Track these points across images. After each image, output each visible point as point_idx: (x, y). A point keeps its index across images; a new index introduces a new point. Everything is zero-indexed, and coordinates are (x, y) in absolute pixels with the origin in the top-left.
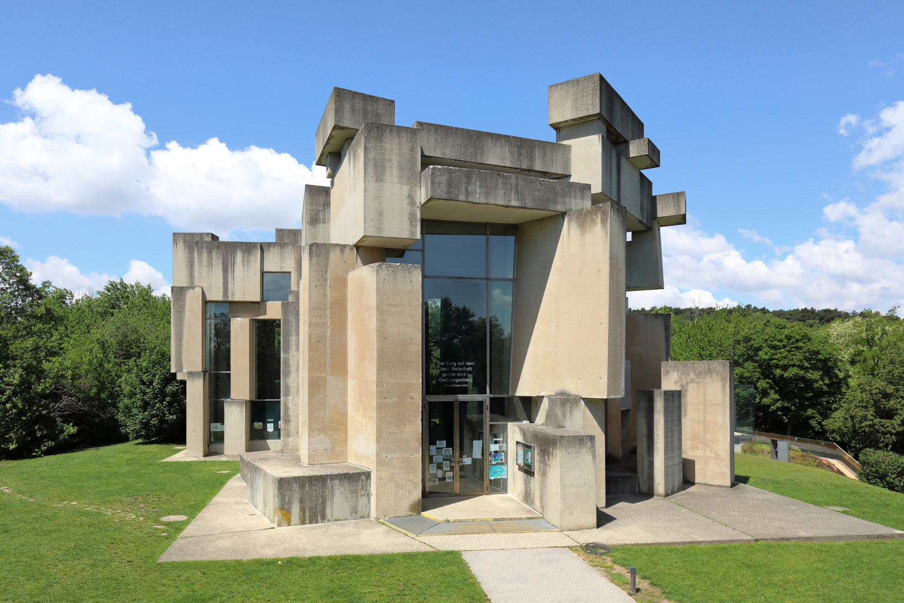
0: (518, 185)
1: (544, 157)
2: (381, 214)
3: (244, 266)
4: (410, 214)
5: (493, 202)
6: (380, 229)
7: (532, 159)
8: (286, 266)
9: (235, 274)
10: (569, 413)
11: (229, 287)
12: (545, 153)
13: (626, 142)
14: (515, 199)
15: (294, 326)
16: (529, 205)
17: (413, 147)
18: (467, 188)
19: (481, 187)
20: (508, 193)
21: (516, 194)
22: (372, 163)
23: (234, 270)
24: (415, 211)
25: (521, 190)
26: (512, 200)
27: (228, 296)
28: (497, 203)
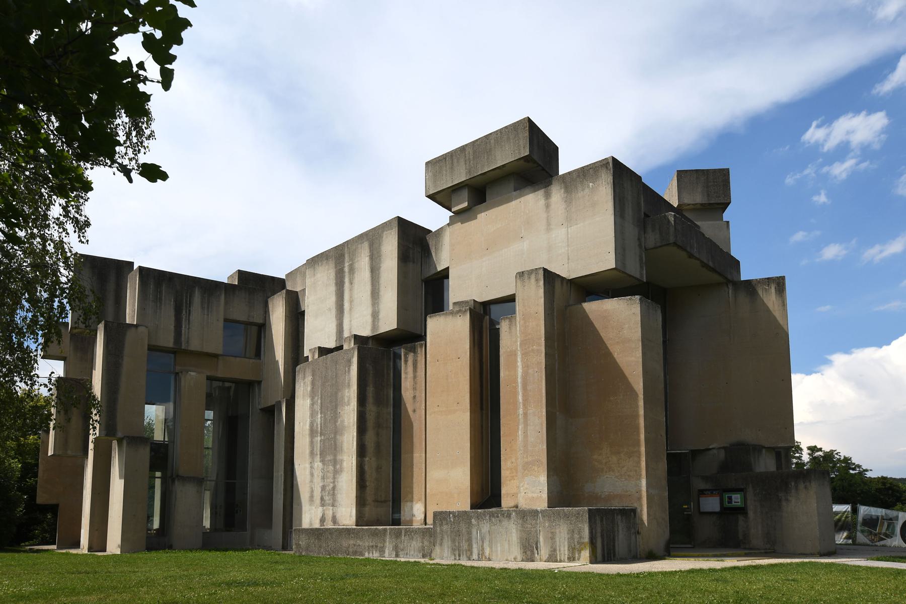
3: (203, 308)
8: (255, 316)
9: (191, 317)
11: (183, 331)
15: (371, 375)
23: (189, 310)
27: (181, 344)
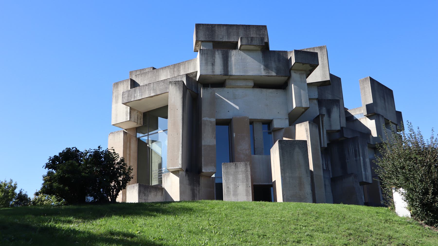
0: (154, 87)
1: (184, 69)
2: (117, 115)
4: (126, 112)
5: (144, 97)
6: (116, 121)
7: (179, 71)
10: (166, 179)
12: (185, 66)
13: (237, 42)
14: (152, 93)
16: (158, 93)
17: (127, 86)
18: (134, 95)
19: (139, 93)
20: (150, 92)
21: (153, 91)
22: (115, 97)
24: (128, 110)
25: (155, 88)
26: (151, 93)
28: (145, 97)
